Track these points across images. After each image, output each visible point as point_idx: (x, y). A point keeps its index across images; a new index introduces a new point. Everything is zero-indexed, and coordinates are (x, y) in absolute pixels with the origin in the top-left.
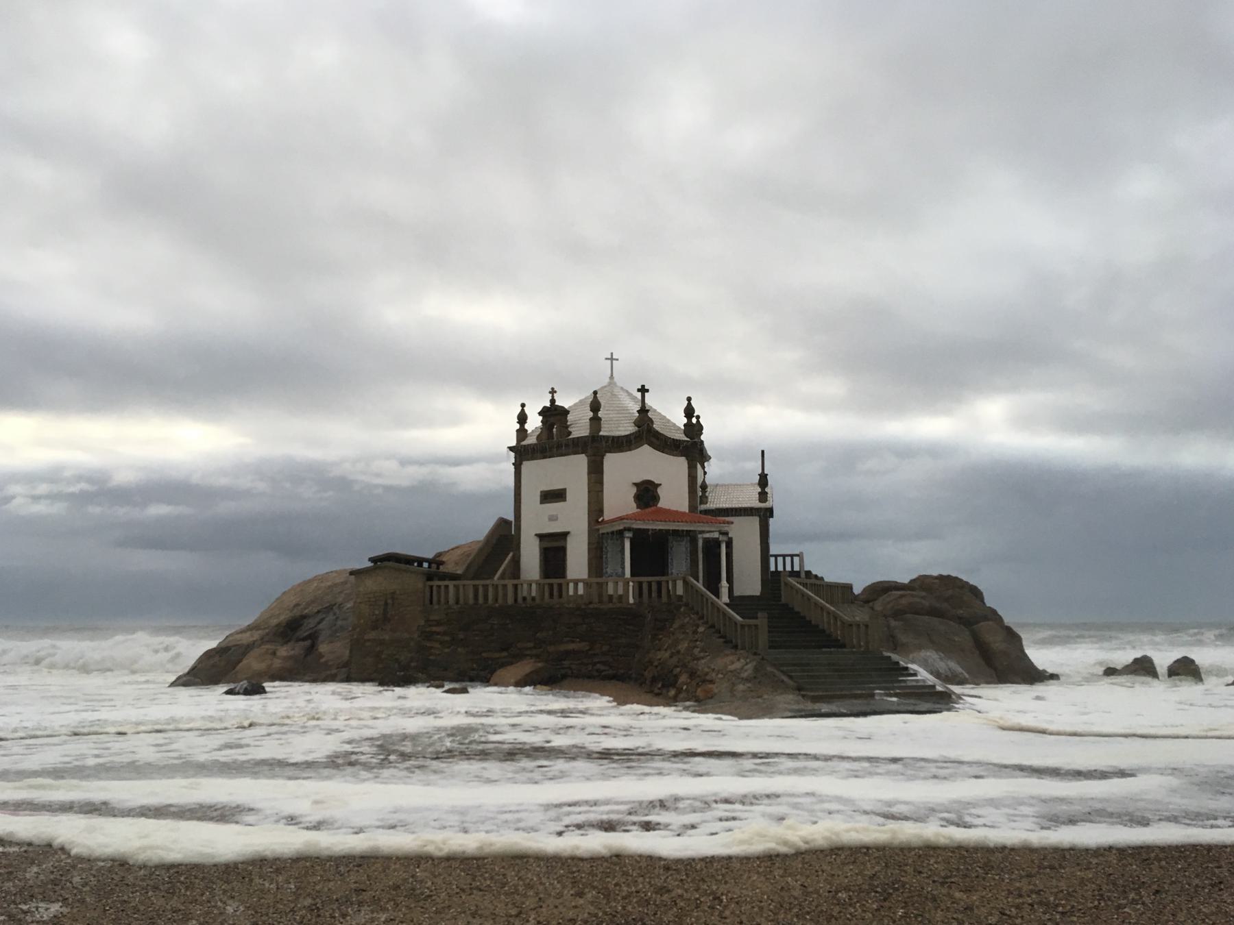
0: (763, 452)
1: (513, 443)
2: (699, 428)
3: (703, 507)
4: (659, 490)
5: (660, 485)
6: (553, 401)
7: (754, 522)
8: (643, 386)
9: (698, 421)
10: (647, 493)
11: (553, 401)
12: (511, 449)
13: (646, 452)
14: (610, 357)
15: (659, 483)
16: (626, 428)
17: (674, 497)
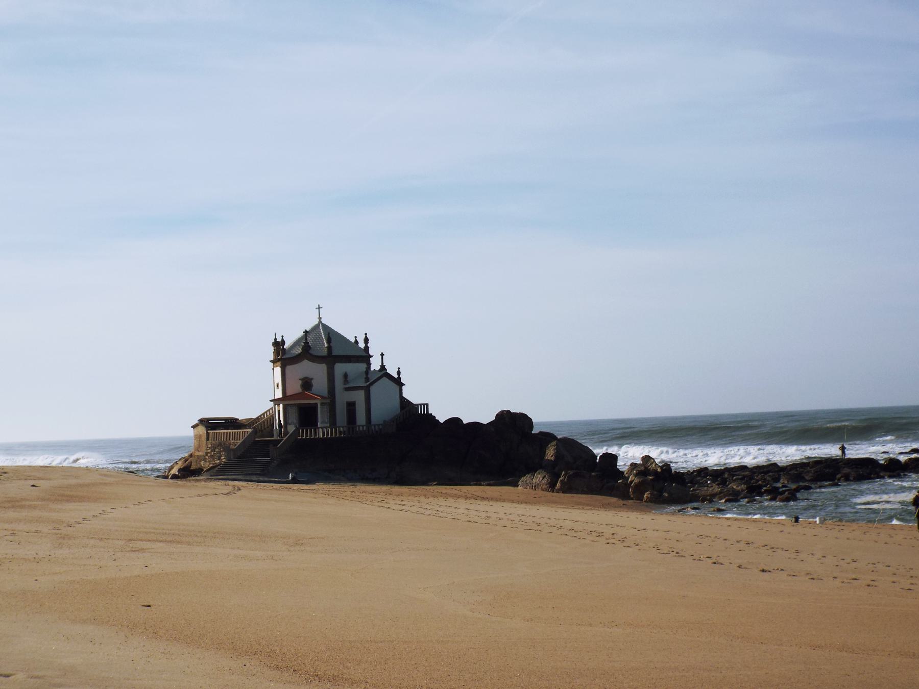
0: (382, 353)
1: (272, 359)
2: (366, 340)
3: (347, 386)
4: (312, 381)
5: (312, 379)
6: (276, 339)
7: (362, 394)
8: (306, 330)
9: (366, 336)
10: (307, 384)
11: (276, 339)
12: (271, 361)
13: (306, 363)
14: (318, 309)
15: (311, 377)
16: (298, 350)
17: (320, 384)
